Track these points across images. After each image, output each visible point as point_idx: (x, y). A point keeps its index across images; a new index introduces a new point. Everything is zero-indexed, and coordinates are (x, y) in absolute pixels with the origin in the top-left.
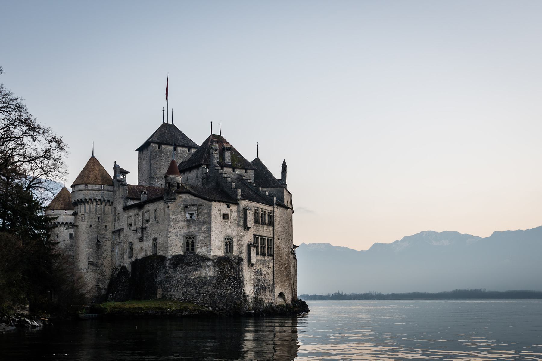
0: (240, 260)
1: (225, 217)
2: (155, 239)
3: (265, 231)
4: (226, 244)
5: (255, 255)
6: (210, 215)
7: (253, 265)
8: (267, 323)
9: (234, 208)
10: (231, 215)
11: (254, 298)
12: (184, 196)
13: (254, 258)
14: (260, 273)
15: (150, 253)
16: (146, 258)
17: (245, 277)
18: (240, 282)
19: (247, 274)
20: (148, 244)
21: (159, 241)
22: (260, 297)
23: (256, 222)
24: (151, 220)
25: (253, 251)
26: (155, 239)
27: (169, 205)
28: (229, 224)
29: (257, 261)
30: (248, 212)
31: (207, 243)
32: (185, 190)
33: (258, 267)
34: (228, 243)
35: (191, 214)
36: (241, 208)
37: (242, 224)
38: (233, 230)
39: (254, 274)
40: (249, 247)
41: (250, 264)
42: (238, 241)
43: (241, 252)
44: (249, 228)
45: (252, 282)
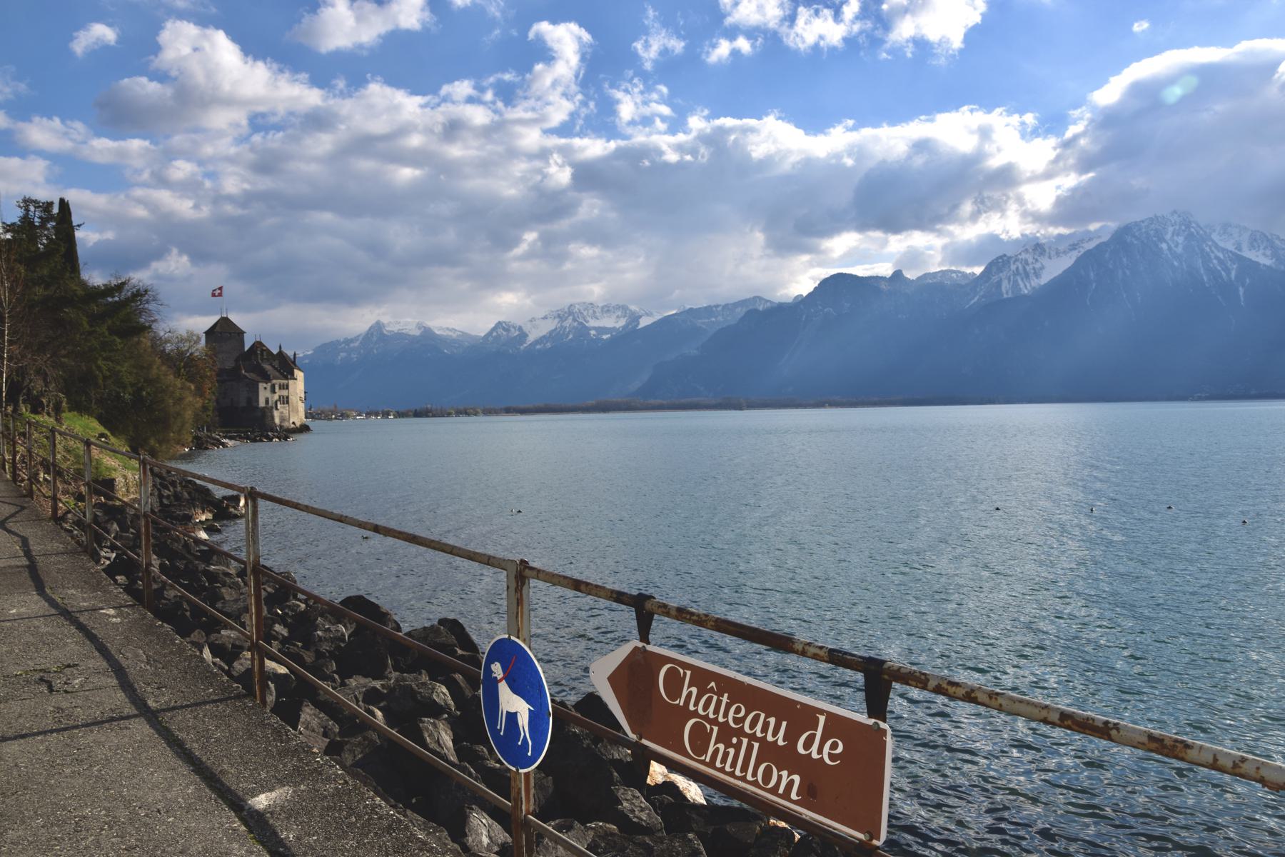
0: (272, 407)
1: (265, 388)
3: (285, 393)
6: (258, 388)
9: (269, 384)
14: (282, 413)
18: (273, 418)
19: (276, 414)
23: (280, 388)
25: (278, 403)
31: (257, 401)
33: (281, 410)
34: (267, 401)
38: (268, 394)
40: (276, 402)
41: (277, 409)
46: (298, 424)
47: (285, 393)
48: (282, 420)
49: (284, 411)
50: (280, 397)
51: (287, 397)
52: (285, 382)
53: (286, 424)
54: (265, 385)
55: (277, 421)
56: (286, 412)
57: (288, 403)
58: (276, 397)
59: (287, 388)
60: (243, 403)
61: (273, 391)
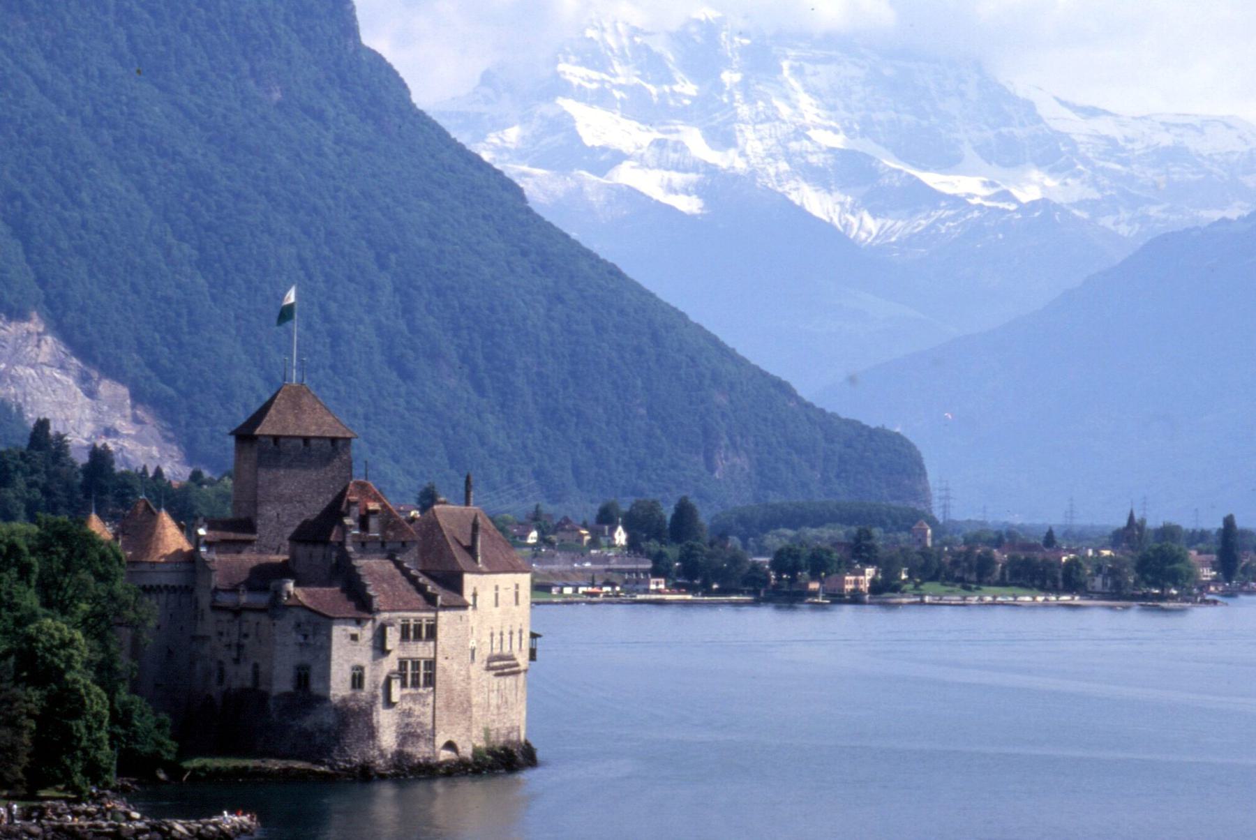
1: (354, 637)
2: (256, 666)
4: (354, 677)
5: (399, 689)
7: (394, 705)
8: (420, 789)
10: (362, 634)
11: (396, 751)
12: (295, 611)
13: (396, 692)
15: (248, 684)
16: (244, 690)
17: (381, 722)
20: (246, 670)
21: (263, 668)
22: (409, 749)
24: (251, 637)
26: (256, 666)
27: (275, 621)
28: (358, 647)
29: (403, 697)
30: (388, 629)
32: (296, 603)
35: (306, 637)
36: (378, 623)
37: (378, 645)
38: (363, 655)
39: (396, 717)
41: (389, 704)
42: (372, 670)
43: (376, 687)
44: (389, 652)
45: (394, 728)
46: (466, 751)
47: (421, 650)
48: (407, 734)
49: (417, 709)
50: (403, 663)
51: (431, 664)
52: (426, 616)
53: (420, 751)
54: (353, 629)
55: (388, 739)
56: (423, 713)
57: (430, 681)
58: (390, 664)
59: (432, 633)
60: (282, 683)
61: (380, 649)
